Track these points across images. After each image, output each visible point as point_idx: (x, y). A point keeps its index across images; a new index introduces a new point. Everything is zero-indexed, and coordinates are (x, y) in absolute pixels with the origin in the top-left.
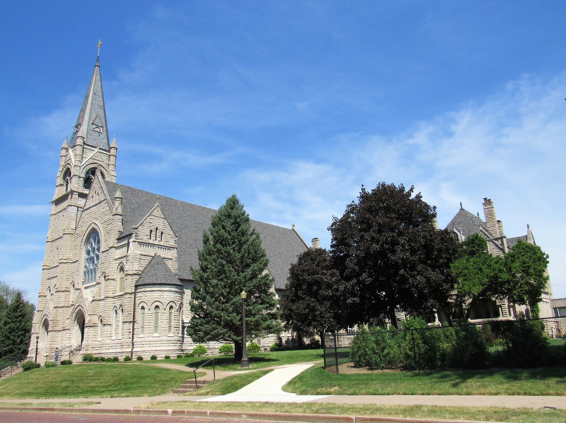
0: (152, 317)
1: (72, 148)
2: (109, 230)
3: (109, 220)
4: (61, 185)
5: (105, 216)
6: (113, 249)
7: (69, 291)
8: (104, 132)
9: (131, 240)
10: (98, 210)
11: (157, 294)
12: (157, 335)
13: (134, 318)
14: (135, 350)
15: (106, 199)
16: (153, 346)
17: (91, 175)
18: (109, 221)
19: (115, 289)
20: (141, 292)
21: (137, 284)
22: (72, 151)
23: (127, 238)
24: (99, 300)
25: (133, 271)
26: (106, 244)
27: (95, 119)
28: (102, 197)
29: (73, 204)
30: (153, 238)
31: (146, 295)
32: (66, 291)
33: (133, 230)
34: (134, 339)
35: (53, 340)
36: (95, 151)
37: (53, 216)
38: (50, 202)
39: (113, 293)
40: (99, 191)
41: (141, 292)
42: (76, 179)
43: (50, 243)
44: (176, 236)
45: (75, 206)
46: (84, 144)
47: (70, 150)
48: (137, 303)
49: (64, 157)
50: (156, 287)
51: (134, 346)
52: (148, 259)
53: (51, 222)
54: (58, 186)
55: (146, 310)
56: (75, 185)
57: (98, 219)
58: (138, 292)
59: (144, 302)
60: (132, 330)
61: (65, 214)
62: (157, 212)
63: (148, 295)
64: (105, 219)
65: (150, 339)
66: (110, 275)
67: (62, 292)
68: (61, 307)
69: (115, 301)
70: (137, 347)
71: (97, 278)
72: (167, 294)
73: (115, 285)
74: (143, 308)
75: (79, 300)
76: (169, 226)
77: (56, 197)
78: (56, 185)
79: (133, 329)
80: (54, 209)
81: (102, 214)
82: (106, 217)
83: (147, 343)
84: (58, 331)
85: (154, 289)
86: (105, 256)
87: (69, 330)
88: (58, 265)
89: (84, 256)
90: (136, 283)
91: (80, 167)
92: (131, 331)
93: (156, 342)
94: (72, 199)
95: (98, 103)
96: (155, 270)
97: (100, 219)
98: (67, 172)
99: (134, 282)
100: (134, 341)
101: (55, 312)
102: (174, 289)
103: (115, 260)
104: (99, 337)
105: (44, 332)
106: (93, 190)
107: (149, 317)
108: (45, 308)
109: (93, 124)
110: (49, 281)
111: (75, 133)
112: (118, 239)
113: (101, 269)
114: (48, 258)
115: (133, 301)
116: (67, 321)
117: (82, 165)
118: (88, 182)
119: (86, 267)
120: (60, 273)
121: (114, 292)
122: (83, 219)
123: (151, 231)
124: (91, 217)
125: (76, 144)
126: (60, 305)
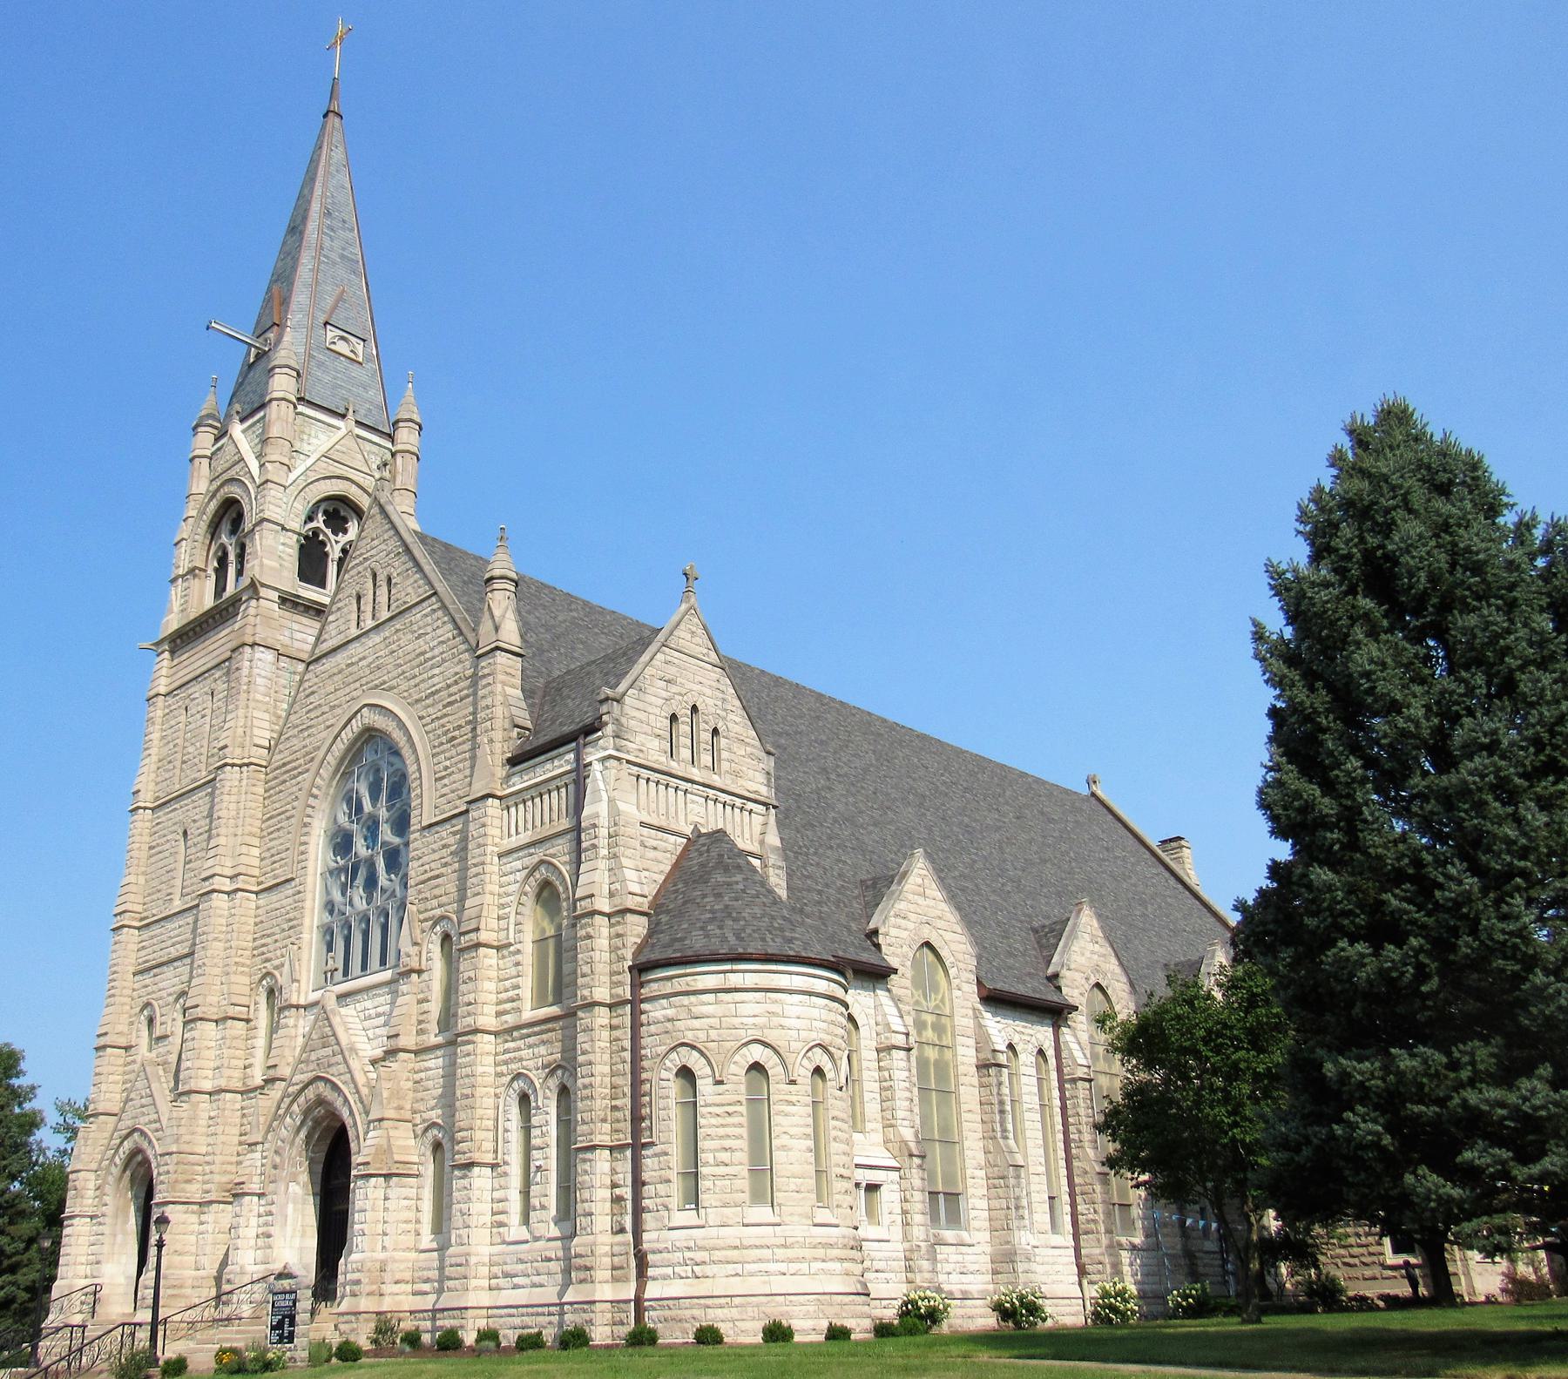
1: (242, 421)
2: (460, 727)
3: (456, 683)
9: (592, 756)
10: (394, 647)
11: (750, 1005)
13: (636, 1132)
14: (652, 1291)
15: (435, 593)
18: (453, 689)
19: (511, 994)
21: (642, 959)
22: (244, 431)
25: (617, 900)
27: (335, 307)
28: (410, 590)
30: (685, 753)
34: (645, 1236)
38: (145, 645)
40: (399, 566)
44: (769, 753)
46: (300, 399)
47: (237, 429)
48: (652, 1045)
51: (651, 1272)
52: (670, 847)
55: (704, 1086)
59: (693, 1047)
60: (629, 1190)
64: (436, 680)
65: (732, 1234)
66: (482, 926)
73: (513, 971)
74: (686, 1073)
75: (313, 1056)
76: (737, 703)
77: (173, 622)
79: (638, 1183)
81: (414, 663)
82: (436, 671)
83: (717, 1255)
85: (735, 980)
86: (444, 846)
89: (318, 854)
92: (627, 1192)
93: (767, 1253)
96: (719, 896)
97: (403, 687)
99: (629, 956)
100: (645, 1246)
102: (821, 986)
106: (360, 568)
107: (720, 1121)
108: (128, 1100)
110: (147, 979)
111: (251, 366)
112: (513, 762)
113: (422, 907)
115: (627, 1044)
117: (290, 482)
118: (312, 561)
119: (330, 907)
121: (508, 1006)
122: (312, 699)
123: (674, 718)
124: (358, 684)
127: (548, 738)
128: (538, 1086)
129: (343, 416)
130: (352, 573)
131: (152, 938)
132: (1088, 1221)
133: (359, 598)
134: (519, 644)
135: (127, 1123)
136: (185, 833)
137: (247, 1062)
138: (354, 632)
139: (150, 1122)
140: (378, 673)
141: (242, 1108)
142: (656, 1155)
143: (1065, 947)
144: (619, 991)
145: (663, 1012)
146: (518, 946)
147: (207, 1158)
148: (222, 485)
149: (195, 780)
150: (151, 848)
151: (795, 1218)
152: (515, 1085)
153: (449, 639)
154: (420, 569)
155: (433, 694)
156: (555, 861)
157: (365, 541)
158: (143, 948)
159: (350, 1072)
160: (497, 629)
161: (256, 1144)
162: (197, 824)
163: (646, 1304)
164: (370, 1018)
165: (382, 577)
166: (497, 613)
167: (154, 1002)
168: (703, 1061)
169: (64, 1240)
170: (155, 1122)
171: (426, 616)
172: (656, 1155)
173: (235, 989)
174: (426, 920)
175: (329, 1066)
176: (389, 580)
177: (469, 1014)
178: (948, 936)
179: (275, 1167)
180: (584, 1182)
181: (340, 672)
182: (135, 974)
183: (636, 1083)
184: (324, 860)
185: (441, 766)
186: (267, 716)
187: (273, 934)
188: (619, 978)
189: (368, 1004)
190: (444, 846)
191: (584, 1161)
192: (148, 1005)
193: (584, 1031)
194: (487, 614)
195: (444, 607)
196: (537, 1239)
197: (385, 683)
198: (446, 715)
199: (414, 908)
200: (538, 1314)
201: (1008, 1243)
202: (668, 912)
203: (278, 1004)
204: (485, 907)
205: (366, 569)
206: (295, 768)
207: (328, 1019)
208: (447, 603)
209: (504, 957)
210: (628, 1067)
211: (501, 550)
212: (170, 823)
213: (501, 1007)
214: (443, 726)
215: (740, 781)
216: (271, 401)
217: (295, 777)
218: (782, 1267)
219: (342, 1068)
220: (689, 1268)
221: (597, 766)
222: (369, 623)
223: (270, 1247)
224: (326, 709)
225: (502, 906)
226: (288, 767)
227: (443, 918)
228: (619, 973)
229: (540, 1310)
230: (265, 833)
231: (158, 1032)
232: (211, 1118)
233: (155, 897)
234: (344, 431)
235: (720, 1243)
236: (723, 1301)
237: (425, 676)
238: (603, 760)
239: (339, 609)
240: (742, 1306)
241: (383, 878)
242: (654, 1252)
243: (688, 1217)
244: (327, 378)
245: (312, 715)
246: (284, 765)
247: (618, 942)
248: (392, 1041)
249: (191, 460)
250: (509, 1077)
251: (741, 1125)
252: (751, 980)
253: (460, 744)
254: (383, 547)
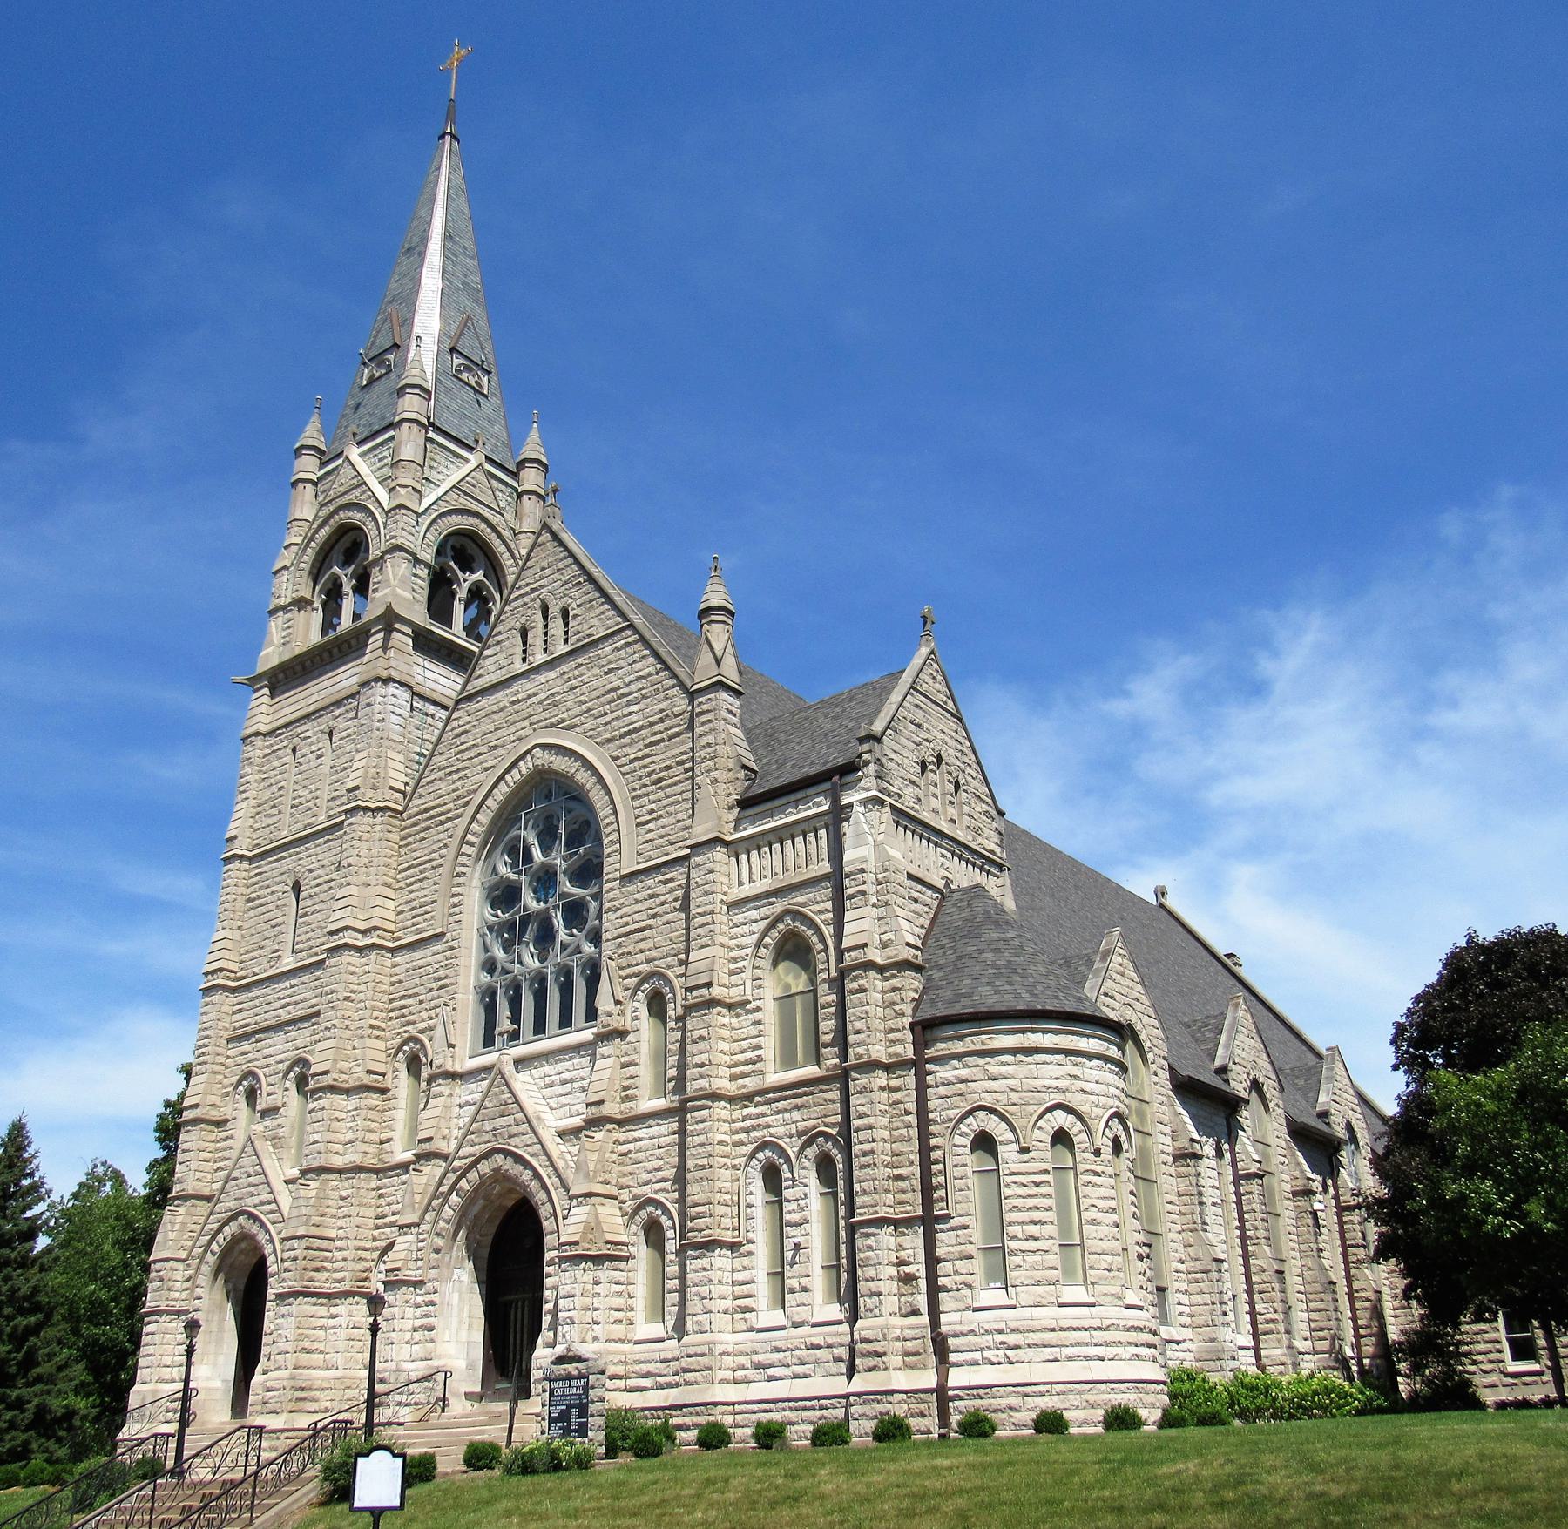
0: (1044, 1190)
1: (359, 443)
2: (668, 768)
3: (662, 720)
4: (301, 603)
5: (629, 704)
6: (720, 854)
7: (384, 1091)
8: (494, 394)
11: (1052, 1070)
12: (1077, 1293)
13: (928, 1202)
14: (956, 1378)
16: (1070, 1359)
17: (452, 563)
18: (656, 728)
20: (959, 1056)
21: (926, 1013)
22: (362, 455)
23: (827, 786)
24: (621, 1123)
25: (890, 951)
26: (649, 836)
28: (594, 621)
29: (394, 675)
31: (994, 1070)
32: (368, 1088)
33: (866, 747)
34: (943, 1318)
35: (307, 1344)
36: (467, 461)
37: (259, 741)
38: (240, 678)
39: (734, 1078)
41: (959, 1056)
42: (405, 565)
43: (245, 865)
45: (402, 684)
49: (308, 486)
50: (1044, 1031)
51: (952, 1357)
53: (249, 770)
54: (284, 608)
55: (1007, 1152)
56: (400, 591)
57: (572, 727)
58: (941, 1060)
59: (992, 1111)
61: (341, 724)
62: (931, 681)
63: (1003, 1069)
64: (633, 718)
65: (1048, 1315)
67: (348, 1092)
68: (340, 1172)
69: (764, 1115)
70: (975, 1363)
71: (604, 1003)
72: (1097, 1075)
73: (753, 1031)
75: (488, 1126)
77: (271, 656)
78: (272, 607)
79: (932, 1260)
80: (263, 708)
82: (634, 708)
84: (329, 1296)
85: (1035, 1039)
86: (652, 896)
87: (418, 1284)
88: (323, 961)
89: (475, 910)
90: (915, 1010)
91: (419, 515)
92: (919, 1269)
94: (392, 653)
95: (465, 276)
98: (332, 547)
99: (908, 1008)
100: (944, 1329)
101: (317, 1197)
103: (731, 906)
104: (640, 1315)
105: (221, 1309)
106: (520, 602)
109: (453, 350)
112: (745, 804)
113: (623, 961)
114: (237, 935)
115: (912, 1107)
116: (405, 1243)
119: (490, 966)
120: (340, 996)
122: (463, 739)
124: (526, 723)
125: (397, 419)
126: (338, 1162)
127: (776, 784)
128: (793, 1156)
129: (471, 449)
130: (515, 604)
131: (252, 999)
132: (1268, 1321)
133: (524, 633)
134: (738, 681)
135: (227, 1205)
136: (296, 888)
137: (383, 1137)
138: (520, 667)
139: (262, 1203)
140: (556, 711)
141: (379, 1188)
142: (952, 1229)
143: (1229, 1037)
144: (899, 1049)
145: (956, 1073)
146: (758, 1003)
147: (338, 1244)
148: (336, 512)
149: (310, 825)
150: (250, 900)
151: (1108, 1299)
152: (760, 1155)
153: (650, 675)
154: (609, 600)
155: (630, 733)
156: (804, 910)
157: (531, 571)
158: (241, 1011)
159: (540, 1143)
160: (718, 662)
161: (409, 1226)
162: (315, 874)
163: (950, 1393)
164: (552, 1085)
165: (555, 608)
166: (718, 647)
167: (260, 1073)
168: (1004, 1125)
169: (145, 1340)
170: (269, 1203)
171: (618, 649)
172: (952, 1229)
173: (370, 1054)
174: (629, 977)
175: (510, 1137)
176: (565, 613)
177: (702, 1077)
178: (1146, 1020)
179: (437, 1251)
180: (868, 1258)
181: (501, 710)
182: (229, 1040)
183: (925, 1149)
184: (482, 916)
185: (644, 810)
186: (401, 758)
187: (416, 994)
188: (898, 1035)
189: (549, 1069)
190: (652, 896)
191: (868, 1236)
192: (250, 1074)
193: (860, 1092)
194: (706, 647)
195: (643, 640)
196: (796, 1325)
197: (563, 721)
198: (648, 756)
199: (613, 964)
200: (805, 1408)
201: (1213, 1340)
202: (940, 967)
203: (425, 1072)
204: (716, 959)
205: (534, 600)
206: (443, 814)
207: (507, 1085)
208: (647, 635)
209: (738, 1015)
210: (914, 1133)
211: (715, 580)
212: (275, 873)
213: (737, 1070)
214: (645, 767)
215: (980, 840)
216: (403, 420)
217: (442, 823)
218: (1100, 1351)
219: (529, 1138)
220: (1001, 1353)
221: (859, 809)
222: (540, 658)
223: (432, 1341)
224: (481, 749)
225: (735, 960)
226: (432, 813)
227: (652, 974)
228: (898, 1030)
229: (808, 1403)
230: (402, 884)
231: (262, 1103)
232: (342, 1198)
233: (255, 954)
234: (473, 464)
235: (1036, 1324)
236: (1042, 1388)
237: (619, 713)
238: (864, 802)
239: (498, 643)
240: (1064, 1393)
241: (562, 934)
242: (956, 1335)
243: (997, 1297)
244: (454, 406)
245: (464, 756)
246: (427, 810)
247: (895, 997)
248: (594, 1109)
249: (294, 484)
250: (752, 1147)
251: (1049, 1196)
252: (1049, 1040)
253: (669, 786)
254: (557, 576)
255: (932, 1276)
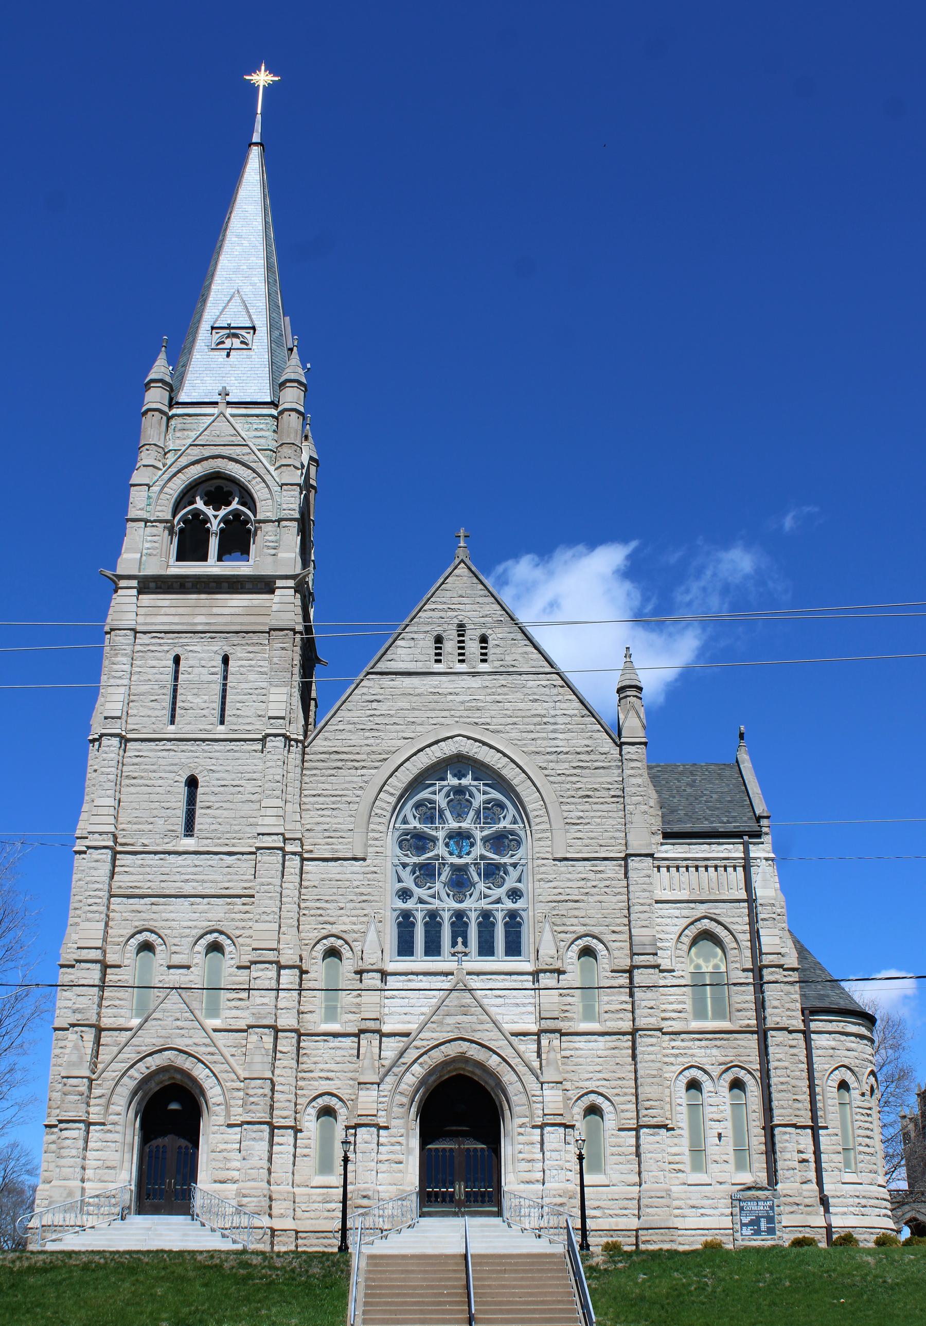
13: (814, 1118)
18: (582, 757)
51: (832, 1209)
70: (845, 1214)
79: (817, 1152)
142: (829, 1135)
163: (833, 1230)
172: (829, 1135)
183: (812, 1086)
188: (793, 1013)
220: (858, 1209)
255: (818, 1161)
